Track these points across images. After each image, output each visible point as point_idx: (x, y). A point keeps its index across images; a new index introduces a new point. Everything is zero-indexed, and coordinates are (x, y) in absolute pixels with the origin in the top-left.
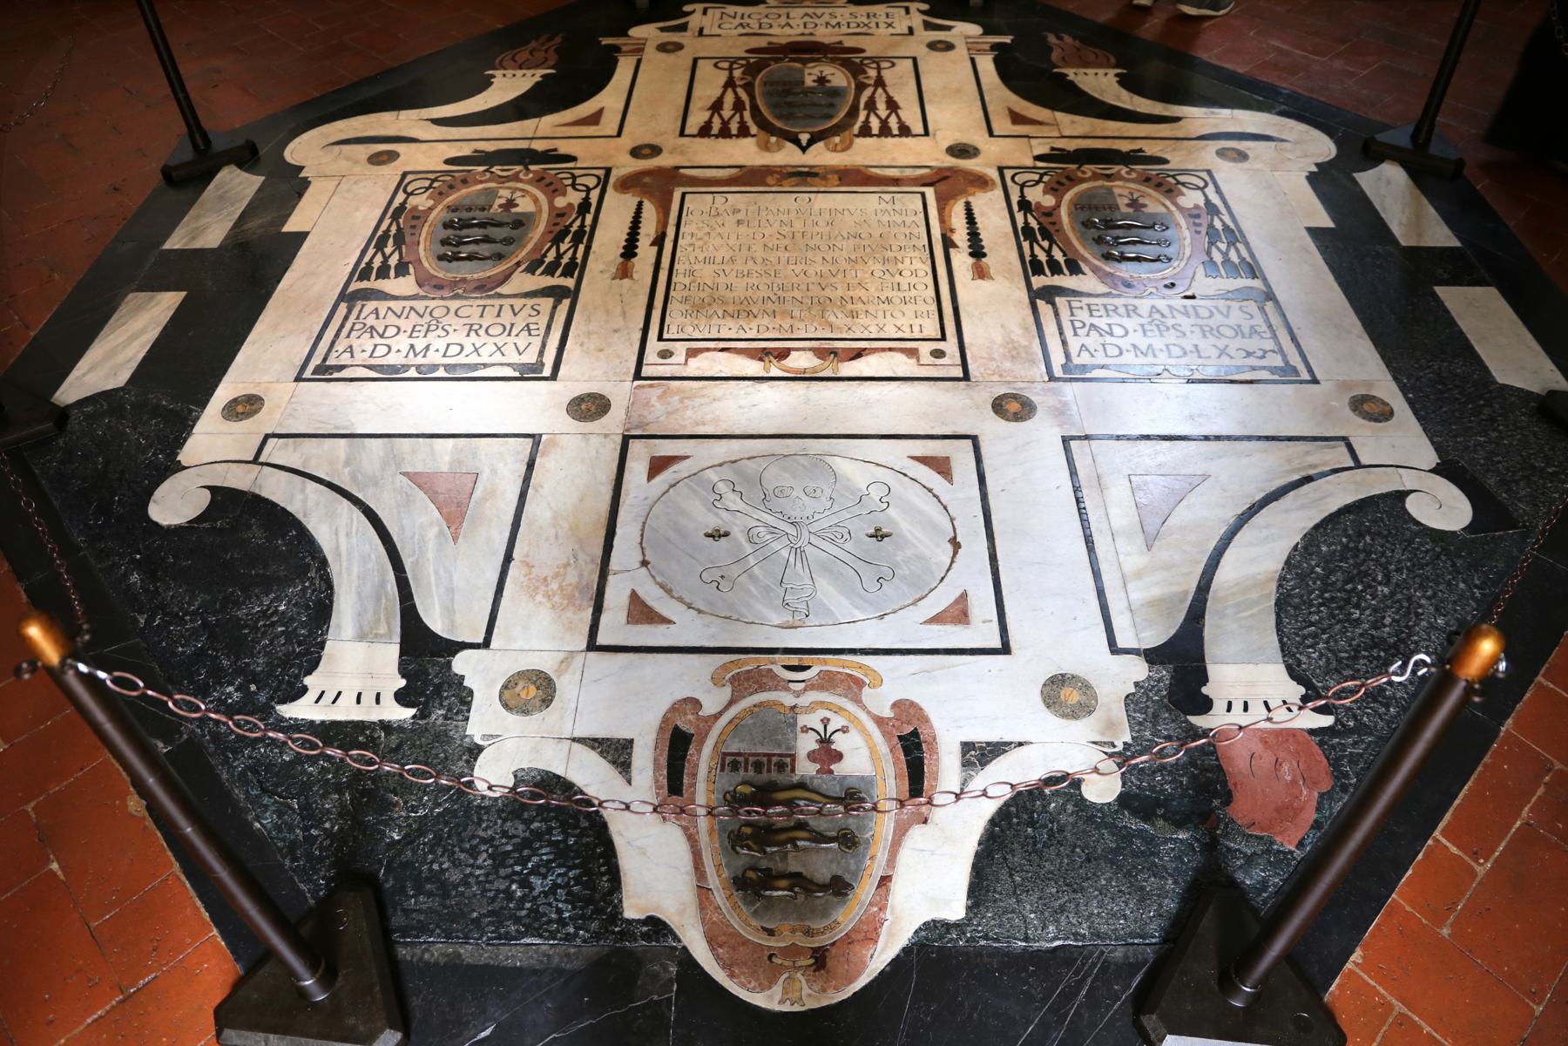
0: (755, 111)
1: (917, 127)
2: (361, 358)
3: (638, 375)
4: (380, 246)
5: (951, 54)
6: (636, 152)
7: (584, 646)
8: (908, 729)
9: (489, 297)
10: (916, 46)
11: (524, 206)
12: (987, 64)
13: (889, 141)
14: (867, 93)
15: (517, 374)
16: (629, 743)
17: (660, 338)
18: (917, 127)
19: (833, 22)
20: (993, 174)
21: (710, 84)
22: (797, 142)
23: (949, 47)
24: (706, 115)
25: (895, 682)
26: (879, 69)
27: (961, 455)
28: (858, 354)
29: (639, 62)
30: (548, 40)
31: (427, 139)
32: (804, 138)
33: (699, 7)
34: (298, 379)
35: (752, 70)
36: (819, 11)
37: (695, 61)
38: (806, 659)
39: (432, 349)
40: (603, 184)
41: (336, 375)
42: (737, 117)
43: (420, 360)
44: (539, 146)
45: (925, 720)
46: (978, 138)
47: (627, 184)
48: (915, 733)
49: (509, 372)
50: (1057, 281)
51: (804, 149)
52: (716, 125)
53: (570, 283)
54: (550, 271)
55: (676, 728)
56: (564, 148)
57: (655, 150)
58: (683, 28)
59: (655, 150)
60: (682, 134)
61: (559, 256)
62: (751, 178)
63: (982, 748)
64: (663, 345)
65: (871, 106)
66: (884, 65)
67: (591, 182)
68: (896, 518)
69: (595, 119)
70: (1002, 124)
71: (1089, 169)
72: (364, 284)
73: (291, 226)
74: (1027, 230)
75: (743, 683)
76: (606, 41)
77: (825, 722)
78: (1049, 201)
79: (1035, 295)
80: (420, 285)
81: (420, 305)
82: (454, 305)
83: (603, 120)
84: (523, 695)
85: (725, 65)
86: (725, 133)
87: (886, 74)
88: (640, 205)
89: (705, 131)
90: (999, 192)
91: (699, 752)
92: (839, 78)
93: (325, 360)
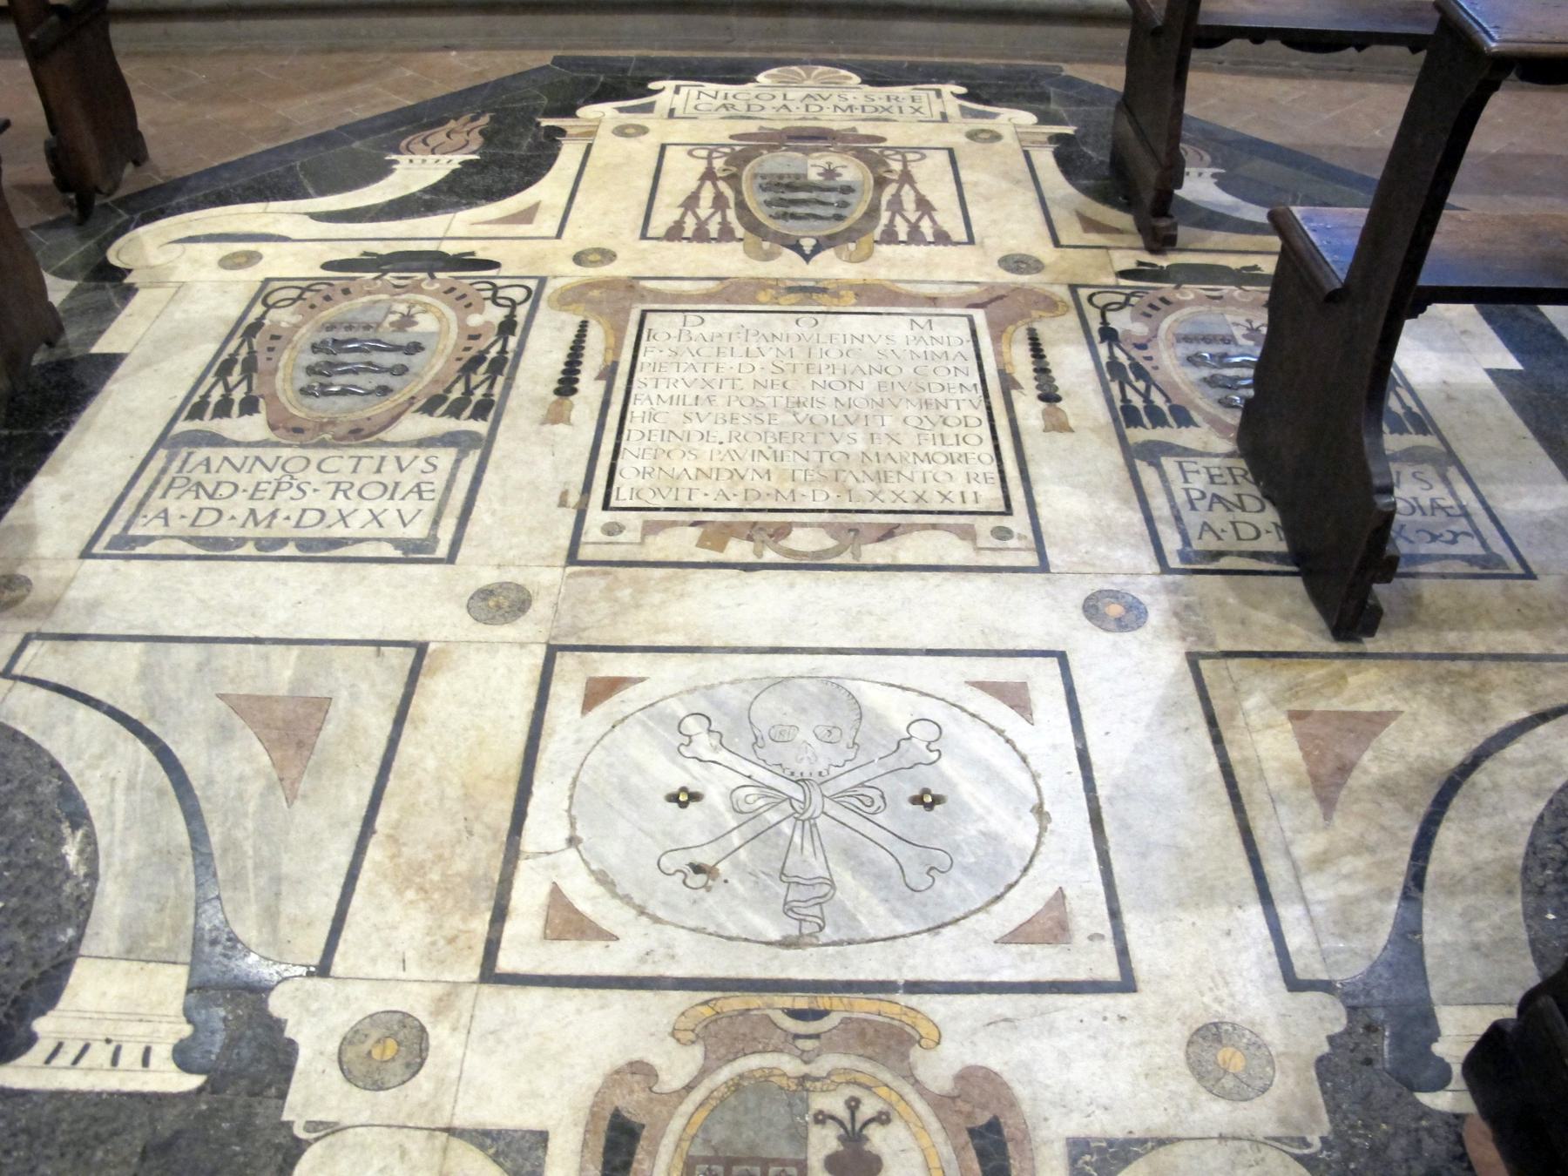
0: (741, 206)
2: (178, 526)
3: (572, 558)
4: (225, 369)
5: (997, 145)
6: (579, 259)
7: (475, 974)
8: (983, 1118)
9: (368, 445)
10: (953, 135)
11: (426, 324)
12: (1045, 159)
13: (914, 250)
14: (889, 191)
15: (398, 554)
16: (542, 1138)
17: (606, 506)
18: (959, 233)
19: (844, 105)
20: (1063, 293)
21: (683, 173)
22: (797, 248)
23: (996, 137)
24: (676, 214)
25: (960, 1040)
26: (905, 162)
27: (1044, 680)
28: (889, 533)
29: (589, 147)
30: (474, 119)
31: (295, 237)
32: (808, 244)
33: (670, 84)
34: (86, 554)
35: (739, 159)
36: (825, 93)
37: (663, 147)
38: (823, 1001)
39: (281, 515)
40: (534, 297)
41: (140, 550)
42: (718, 218)
43: (260, 532)
44: (451, 248)
45: (1013, 1103)
46: (1044, 251)
47: (567, 299)
48: (994, 1126)
49: (389, 551)
50: (1159, 434)
51: (807, 258)
52: (690, 225)
53: (481, 427)
54: (455, 411)
55: (617, 1114)
56: (482, 251)
57: (607, 256)
58: (649, 108)
59: (607, 256)
60: (644, 236)
61: (469, 392)
62: (732, 294)
63: (1100, 1150)
64: (608, 517)
65: (896, 206)
66: (910, 156)
67: (518, 294)
68: (952, 774)
69: (527, 216)
70: (1071, 233)
71: (1190, 292)
72: (196, 425)
73: (101, 347)
74: (1114, 365)
75: (720, 1038)
76: (546, 122)
77: (853, 1105)
78: (1139, 329)
79: (1131, 453)
80: (273, 427)
81: (269, 455)
82: (315, 455)
83: (539, 217)
84: (376, 1054)
85: (704, 153)
86: (701, 235)
87: (917, 171)
88: (583, 326)
90: (1072, 319)
91: (653, 1155)
92: (851, 171)
93: (126, 528)
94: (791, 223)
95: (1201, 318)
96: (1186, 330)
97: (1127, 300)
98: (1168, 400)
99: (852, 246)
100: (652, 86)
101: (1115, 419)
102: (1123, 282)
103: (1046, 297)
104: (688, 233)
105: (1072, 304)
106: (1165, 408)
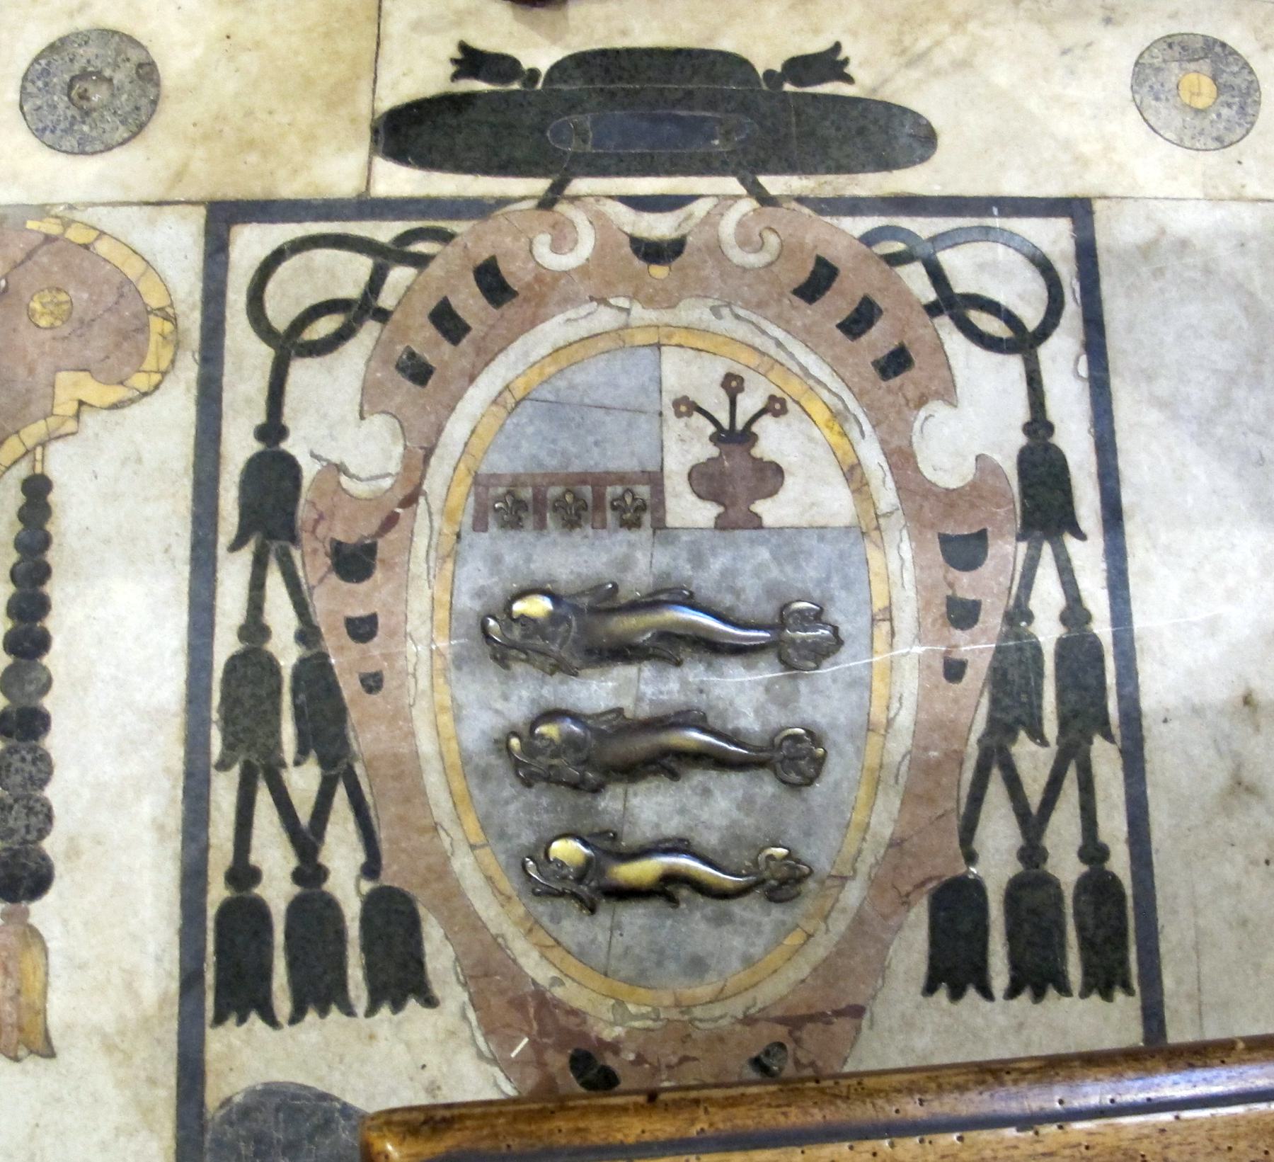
90: (176, 405)
95: (591, 376)
96: (525, 452)
97: (376, 282)
98: (371, 869)
101: (190, 981)
102: (398, 180)
103: (126, 288)
105: (192, 321)
106: (352, 909)
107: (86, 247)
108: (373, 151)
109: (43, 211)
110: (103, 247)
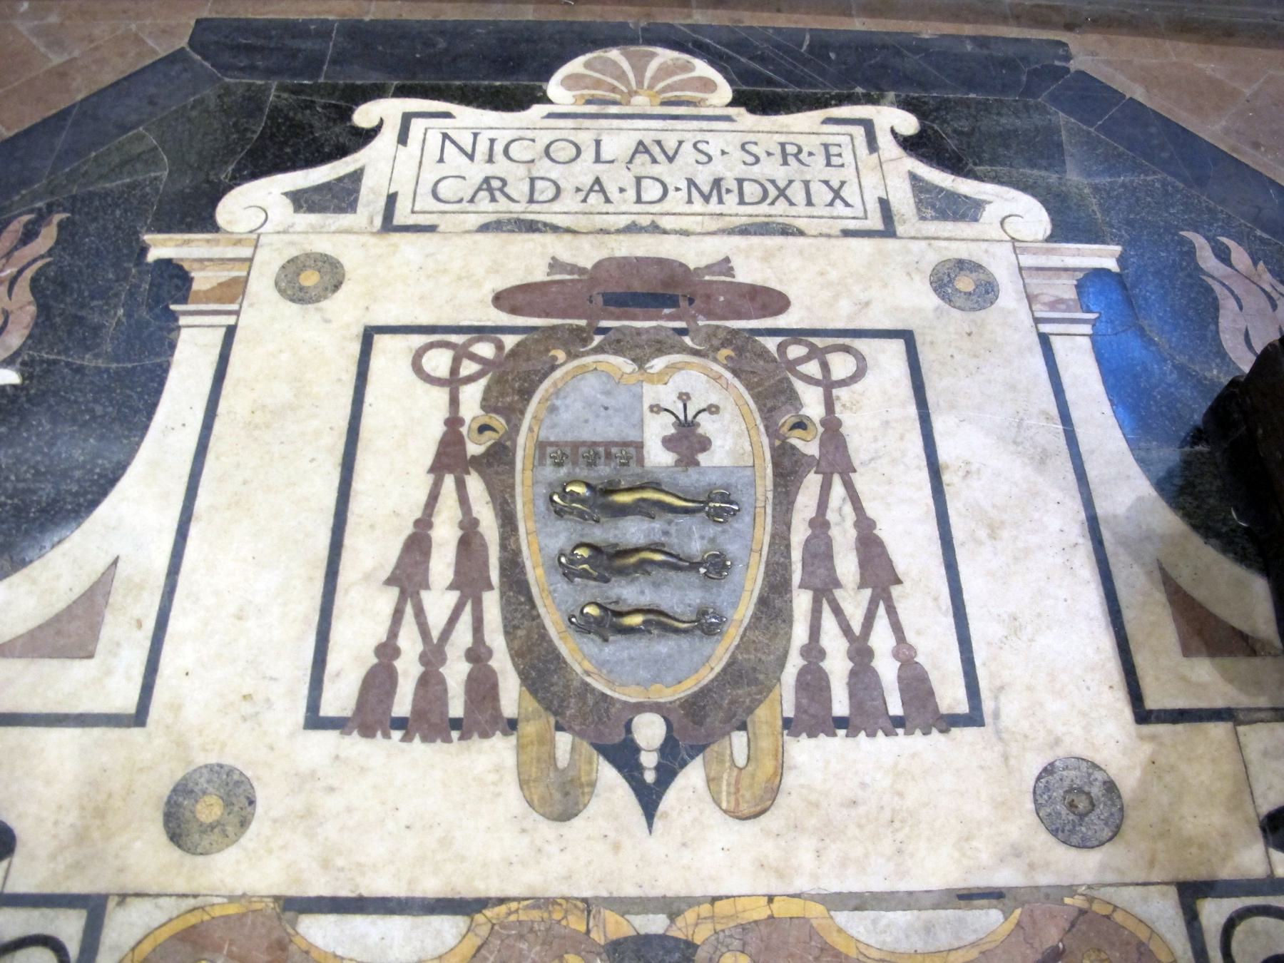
1: (952, 697)
19: (704, 179)
22: (623, 756)
29: (231, 332)
32: (649, 732)
60: (315, 721)
89: (371, 716)
94: (618, 648)
99: (739, 740)
100: (364, 116)
104: (402, 705)
107: (1108, 917)
108: (1267, 844)
109: (1071, 890)
110: (1118, 917)
